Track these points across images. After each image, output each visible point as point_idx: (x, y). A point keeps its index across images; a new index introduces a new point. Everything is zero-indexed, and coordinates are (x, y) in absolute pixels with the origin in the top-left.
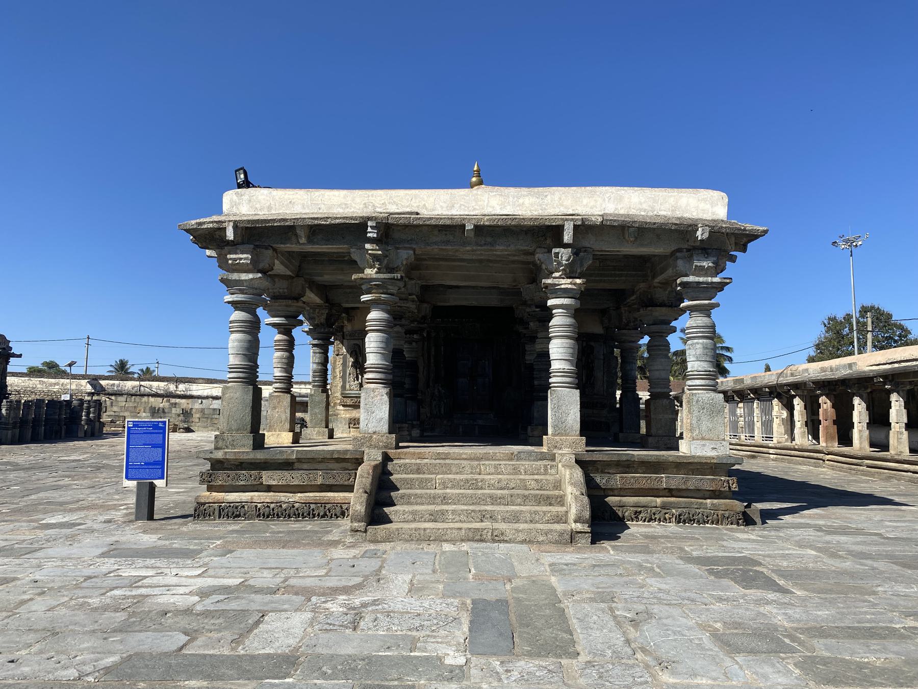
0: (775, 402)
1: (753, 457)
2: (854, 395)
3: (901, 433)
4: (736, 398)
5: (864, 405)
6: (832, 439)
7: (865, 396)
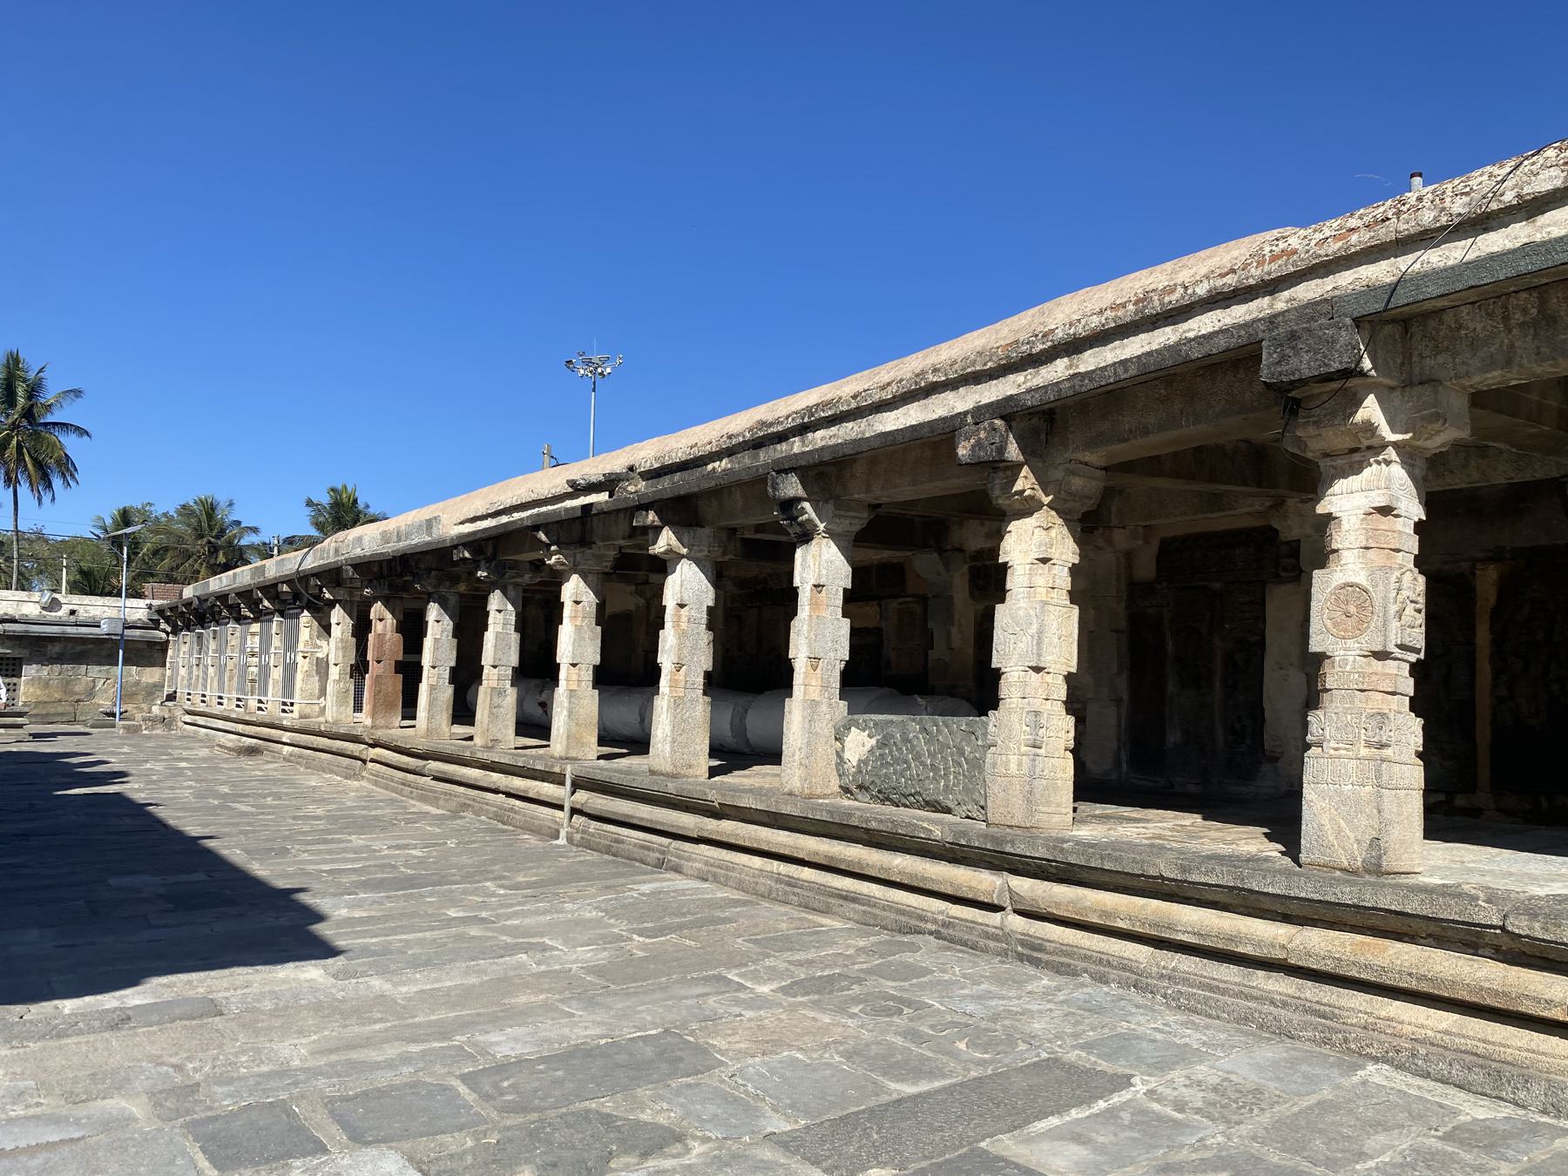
0: (305, 617)
1: (252, 751)
2: (429, 597)
3: (501, 693)
4: (245, 612)
5: (448, 623)
6: (389, 707)
7: (453, 600)
